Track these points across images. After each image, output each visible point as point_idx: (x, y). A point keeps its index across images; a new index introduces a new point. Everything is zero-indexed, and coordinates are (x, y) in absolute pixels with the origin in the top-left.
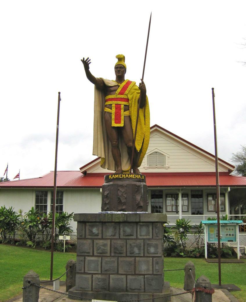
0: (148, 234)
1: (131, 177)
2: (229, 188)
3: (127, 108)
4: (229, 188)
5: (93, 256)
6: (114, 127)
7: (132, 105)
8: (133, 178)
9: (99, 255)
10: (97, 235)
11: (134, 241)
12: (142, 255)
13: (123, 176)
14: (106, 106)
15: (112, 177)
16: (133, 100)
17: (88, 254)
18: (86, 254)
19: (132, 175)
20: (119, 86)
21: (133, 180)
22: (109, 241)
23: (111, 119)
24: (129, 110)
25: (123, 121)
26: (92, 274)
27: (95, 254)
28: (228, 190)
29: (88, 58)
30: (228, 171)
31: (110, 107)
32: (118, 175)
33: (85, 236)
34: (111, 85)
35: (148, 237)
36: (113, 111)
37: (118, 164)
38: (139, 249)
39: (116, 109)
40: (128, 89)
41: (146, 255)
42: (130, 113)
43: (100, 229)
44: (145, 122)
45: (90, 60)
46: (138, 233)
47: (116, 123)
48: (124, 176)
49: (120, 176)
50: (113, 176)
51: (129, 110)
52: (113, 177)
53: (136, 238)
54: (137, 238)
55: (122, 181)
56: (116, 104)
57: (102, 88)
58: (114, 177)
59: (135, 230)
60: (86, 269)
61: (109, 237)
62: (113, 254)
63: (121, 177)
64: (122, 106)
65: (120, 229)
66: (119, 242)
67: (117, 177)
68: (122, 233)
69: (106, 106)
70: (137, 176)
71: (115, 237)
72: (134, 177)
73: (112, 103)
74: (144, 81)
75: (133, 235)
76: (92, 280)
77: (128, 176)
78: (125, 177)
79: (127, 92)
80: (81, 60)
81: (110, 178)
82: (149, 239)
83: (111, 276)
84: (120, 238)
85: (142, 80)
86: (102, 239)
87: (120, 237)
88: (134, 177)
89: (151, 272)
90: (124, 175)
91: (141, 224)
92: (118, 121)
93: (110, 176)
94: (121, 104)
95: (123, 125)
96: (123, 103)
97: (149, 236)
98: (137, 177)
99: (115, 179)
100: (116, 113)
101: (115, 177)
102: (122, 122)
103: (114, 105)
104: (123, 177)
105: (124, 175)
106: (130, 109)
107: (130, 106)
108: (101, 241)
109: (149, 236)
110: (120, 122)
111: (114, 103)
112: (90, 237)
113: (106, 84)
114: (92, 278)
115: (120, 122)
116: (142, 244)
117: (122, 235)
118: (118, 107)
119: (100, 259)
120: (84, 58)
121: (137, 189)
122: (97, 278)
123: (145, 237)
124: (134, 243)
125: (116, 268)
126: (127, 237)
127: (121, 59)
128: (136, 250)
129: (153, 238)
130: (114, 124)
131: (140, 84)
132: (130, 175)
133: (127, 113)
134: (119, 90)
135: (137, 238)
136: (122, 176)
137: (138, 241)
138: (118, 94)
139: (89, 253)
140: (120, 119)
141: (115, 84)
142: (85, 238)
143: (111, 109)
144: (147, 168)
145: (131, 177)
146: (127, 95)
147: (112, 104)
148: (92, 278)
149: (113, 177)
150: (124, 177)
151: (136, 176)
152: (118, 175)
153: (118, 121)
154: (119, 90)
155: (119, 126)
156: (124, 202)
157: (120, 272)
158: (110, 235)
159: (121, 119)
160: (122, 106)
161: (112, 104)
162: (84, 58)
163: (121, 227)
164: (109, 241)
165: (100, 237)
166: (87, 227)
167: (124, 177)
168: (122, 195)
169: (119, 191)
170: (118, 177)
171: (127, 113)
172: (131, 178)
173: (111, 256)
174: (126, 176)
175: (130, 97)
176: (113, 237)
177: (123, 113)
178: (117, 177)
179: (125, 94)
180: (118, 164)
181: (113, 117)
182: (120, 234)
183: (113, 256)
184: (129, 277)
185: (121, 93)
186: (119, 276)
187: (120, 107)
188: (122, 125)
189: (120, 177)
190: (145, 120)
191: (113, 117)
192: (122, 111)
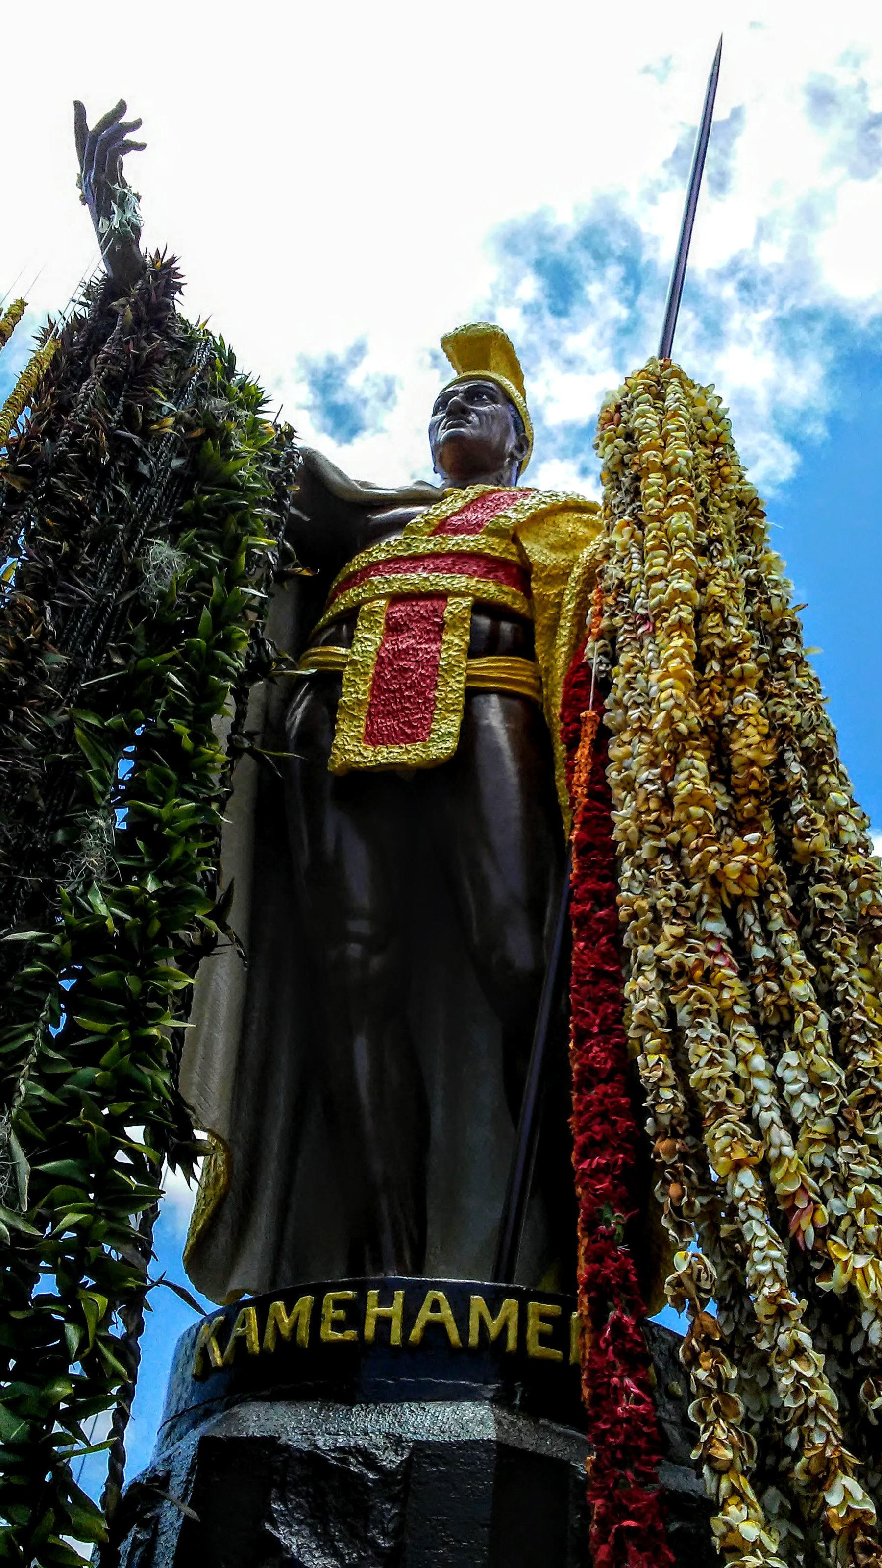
1: (494, 1327)
8: (535, 1349)
13: (374, 1310)
47: (372, 737)
48: (395, 1310)
49: (330, 1313)
63: (338, 1326)
77: (446, 1313)
78: (395, 1336)
88: (544, 1339)
90: (386, 1300)
95: (451, 744)
104: (369, 1331)
105: (386, 1300)
132: (478, 1303)
136: (355, 1314)
145: (494, 1327)
146: (515, 540)
150: (384, 1323)
152: (305, 1302)
167: (384, 1323)
170: (304, 1334)
174: (425, 1315)
189: (328, 1334)
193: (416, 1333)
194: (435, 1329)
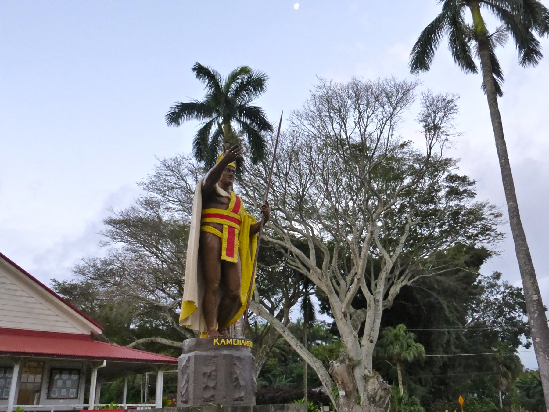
13: (238, 342)
14: (208, 224)
15: (219, 342)
31: (220, 227)
32: (231, 340)
36: (225, 236)
39: (229, 233)
47: (228, 255)
49: (234, 342)
50: (223, 341)
55: (237, 350)
56: (229, 226)
73: (223, 223)
81: (214, 344)
92: (230, 253)
99: (226, 345)
101: (226, 342)
103: (227, 226)
111: (226, 223)
118: (231, 230)
136: (236, 342)
143: (222, 232)
149: (223, 343)
152: (231, 340)
153: (230, 253)
169: (235, 367)
181: (225, 245)
191: (225, 245)
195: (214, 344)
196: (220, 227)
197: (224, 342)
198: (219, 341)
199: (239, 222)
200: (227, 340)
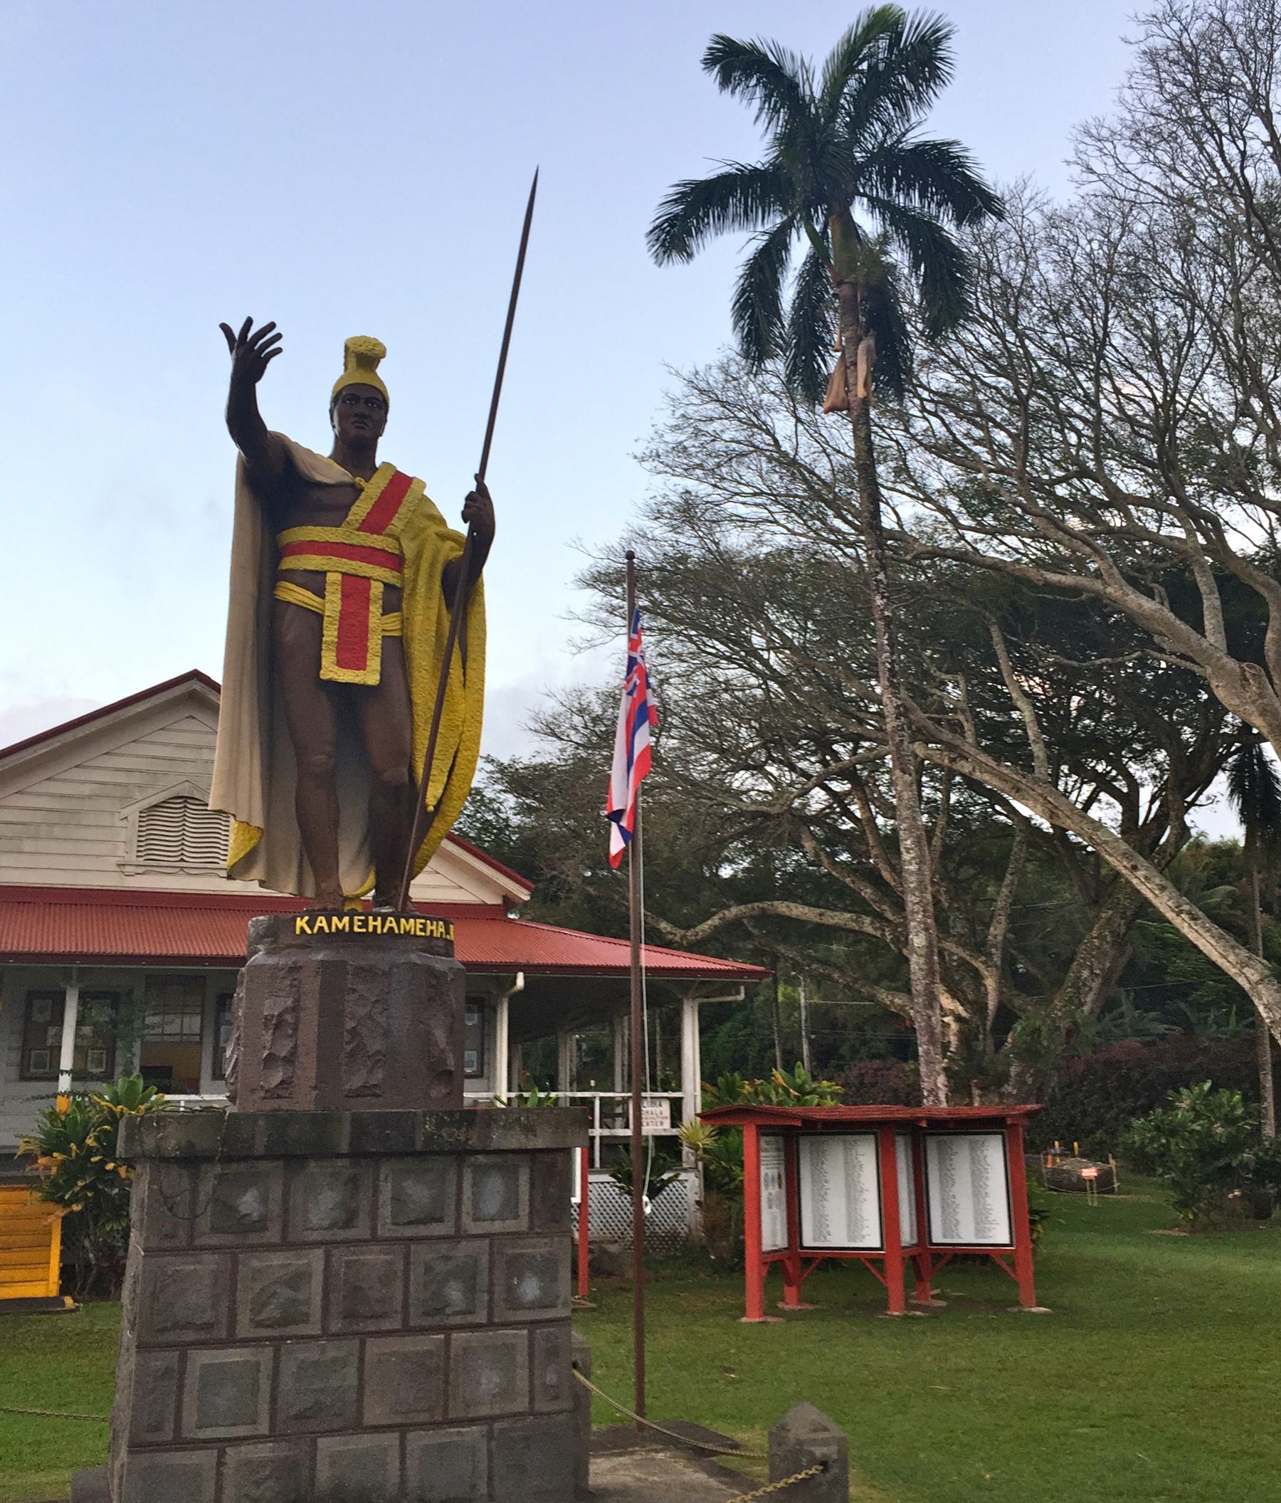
0: (509, 1209)
2: (520, 976)
3: (394, 599)
4: (520, 976)
5: (231, 1341)
6: (331, 683)
7: (414, 588)
8: (419, 933)
9: (264, 1332)
10: (260, 1225)
11: (444, 1247)
12: (481, 1318)
13: (371, 923)
14: (290, 575)
15: (312, 928)
16: (425, 566)
17: (203, 1336)
18: (190, 1336)
19: (412, 921)
20: (357, 491)
21: (414, 940)
22: (320, 1252)
23: (321, 642)
24: (399, 609)
25: (378, 660)
26: (221, 1444)
27: (244, 1329)
28: (515, 984)
29: (272, 326)
30: (498, 901)
31: (315, 582)
32: (346, 919)
33: (192, 1237)
34: (319, 478)
35: (511, 1225)
36: (332, 605)
37: (317, 857)
38: (471, 1290)
39: (345, 596)
40: (402, 510)
41: (502, 1314)
42: (405, 623)
43: (276, 1193)
44: (464, 674)
45: (279, 336)
46: (467, 1206)
47: (341, 663)
48: (379, 923)
49: (357, 923)
50: (321, 922)
51: (399, 609)
52: (318, 924)
53: (452, 1232)
54: (459, 1236)
56: (344, 574)
57: (274, 484)
58: (327, 930)
59: (452, 1190)
60: (190, 1418)
61: (315, 1236)
62: (336, 1326)
63: (359, 927)
64: (376, 589)
65: (376, 1191)
66: (374, 1257)
67: (340, 926)
68: (386, 1211)
69: (290, 575)
70: (434, 928)
71: (352, 1233)
72: (421, 930)
73: (326, 568)
74: (486, 482)
75: (440, 1220)
76: (219, 1474)
77: (394, 925)
78: (379, 931)
79: (397, 524)
80: (225, 328)
81: (298, 932)
82: (516, 1235)
83: (322, 1442)
84: (375, 1239)
85: (480, 477)
86: (286, 1244)
87: (374, 1229)
88: (421, 930)
89: (521, 1405)
90: (375, 920)
91: (481, 1159)
92: (352, 654)
93: (301, 923)
94: (368, 579)
96: (379, 575)
97: (516, 1217)
98: (432, 931)
100: (344, 616)
102: (374, 663)
103: (339, 577)
104: (371, 929)
105: (375, 920)
106: (404, 605)
107: (407, 591)
108: (277, 1259)
109: (516, 1217)
110: (360, 665)
111: (335, 569)
112: (214, 1240)
113: (302, 467)
114: (220, 1464)
115: (359, 663)
116: (485, 1260)
117: (388, 1221)
118: (355, 589)
119: (265, 1356)
120: (249, 322)
121: (434, 986)
122: (248, 1463)
123: (497, 1227)
124: (448, 1258)
125: (353, 1395)
126: (408, 1232)
127: (364, 357)
128: (455, 1293)
129: (531, 1228)
130: (331, 670)
131: (470, 498)
133: (392, 623)
134: (361, 509)
135: (459, 1236)
136: (365, 924)
137: (464, 1248)
138: (358, 530)
139: (208, 1326)
140: (365, 649)
141: (338, 474)
142: (192, 1249)
143: (323, 597)
144: (132, 869)
146: (398, 539)
147: (325, 573)
148: (220, 1464)
150: (375, 927)
151: (429, 928)
152: (346, 919)
153: (352, 654)
154: (361, 509)
155: (357, 680)
156: (378, 1052)
157: (370, 1418)
158: (326, 1223)
159: (366, 646)
160: (376, 589)
161: (325, 573)
162: (249, 322)
163: (382, 1177)
164: (316, 1259)
165: (273, 1235)
166: (207, 1187)
167: (375, 927)
168: (370, 1017)
170: (347, 929)
171: (392, 623)
172: (407, 933)
173: (326, 1334)
174: (388, 925)
175: (409, 549)
176: (341, 1234)
177: (379, 624)
178: (340, 926)
179: (388, 530)
180: (317, 857)
181: (330, 634)
182: (374, 1216)
183: (337, 1336)
184: (418, 1440)
185: (374, 523)
186: (366, 1441)
187: (368, 589)
188: (371, 677)
189: (356, 929)
190: (464, 668)
192: (375, 609)
193: (385, 930)
194: (391, 929)
195: (298, 932)
196: (315, 582)
197: (324, 924)
198: (311, 924)
199: (396, 561)
200: (335, 919)
